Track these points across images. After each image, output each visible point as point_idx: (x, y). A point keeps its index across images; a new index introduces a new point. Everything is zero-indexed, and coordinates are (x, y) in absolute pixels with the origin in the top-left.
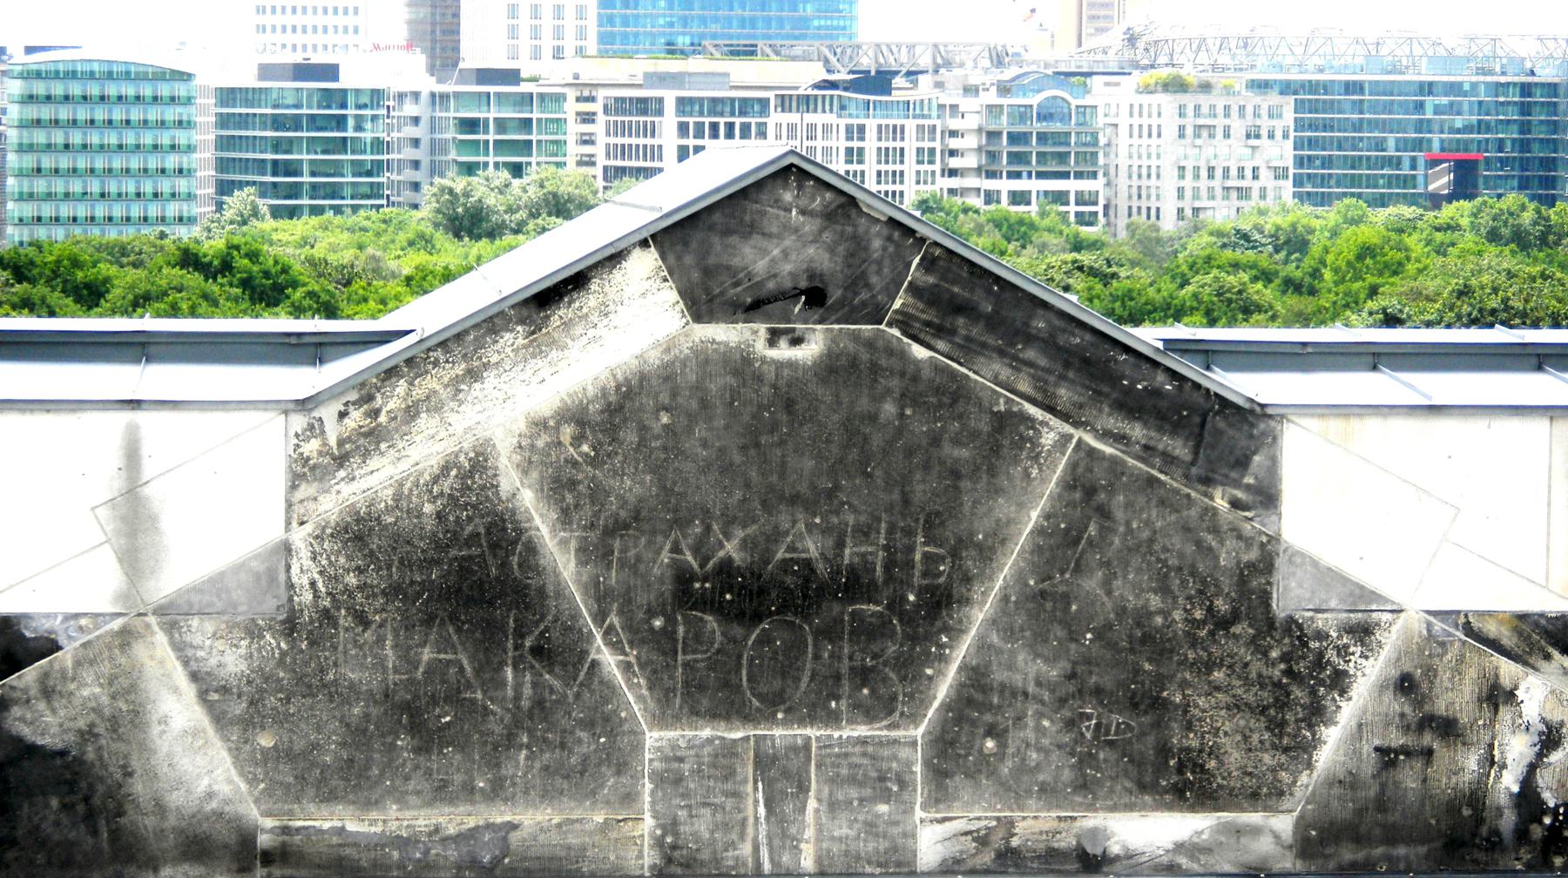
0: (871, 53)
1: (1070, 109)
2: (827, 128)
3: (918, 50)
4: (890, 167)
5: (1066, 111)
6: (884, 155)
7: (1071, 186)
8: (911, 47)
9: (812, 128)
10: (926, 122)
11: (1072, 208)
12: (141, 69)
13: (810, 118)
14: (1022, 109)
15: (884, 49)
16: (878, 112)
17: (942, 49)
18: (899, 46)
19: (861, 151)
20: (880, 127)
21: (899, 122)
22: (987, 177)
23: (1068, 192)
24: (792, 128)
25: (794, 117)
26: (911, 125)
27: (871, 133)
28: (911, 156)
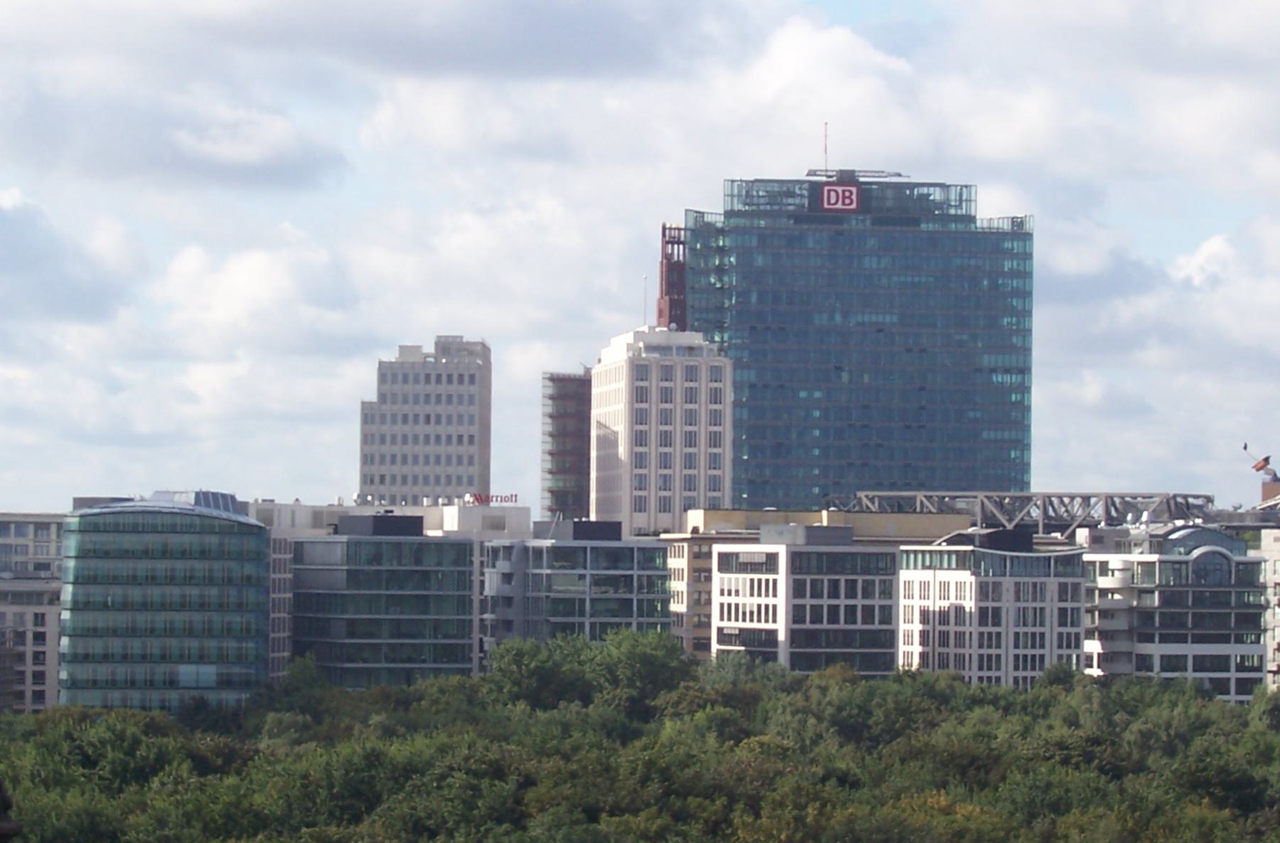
1: (1230, 566)
2: (960, 586)
5: (1225, 567)
6: (1022, 617)
8: (1086, 499)
11: (1233, 675)
12: (207, 522)
13: (943, 575)
14: (1177, 566)
15: (1055, 501)
16: (1015, 568)
17: (1117, 500)
18: (1072, 498)
19: (996, 612)
20: (1017, 584)
21: (1039, 580)
22: (1140, 641)
23: (1186, 656)
24: (924, 586)
25: (927, 575)
26: (1052, 583)
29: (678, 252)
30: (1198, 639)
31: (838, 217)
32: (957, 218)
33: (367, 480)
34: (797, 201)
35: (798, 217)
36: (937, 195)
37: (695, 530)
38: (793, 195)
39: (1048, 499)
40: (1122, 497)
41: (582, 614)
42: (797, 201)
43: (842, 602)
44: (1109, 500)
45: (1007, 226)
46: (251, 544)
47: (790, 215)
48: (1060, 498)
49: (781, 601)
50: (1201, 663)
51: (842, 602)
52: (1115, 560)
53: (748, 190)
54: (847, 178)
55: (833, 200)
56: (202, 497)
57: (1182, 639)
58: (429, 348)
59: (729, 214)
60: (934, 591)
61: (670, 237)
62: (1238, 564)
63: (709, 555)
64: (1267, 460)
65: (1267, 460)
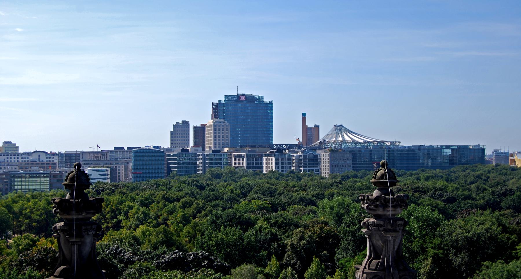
0: (276, 146)
2: (272, 159)
3: (284, 146)
4: (283, 166)
7: (314, 168)
8: (283, 145)
9: (269, 159)
10: (289, 158)
13: (269, 157)
18: (281, 145)
20: (281, 159)
25: (266, 157)
27: (280, 160)
28: (286, 164)
29: (215, 107)
30: (309, 167)
31: (242, 101)
32: (261, 101)
33: (171, 143)
34: (236, 98)
35: (236, 101)
36: (257, 97)
37: (228, 151)
38: (235, 98)
39: (277, 145)
40: (289, 145)
41: (214, 164)
42: (236, 98)
43: (254, 162)
44: (287, 145)
45: (269, 102)
46: (162, 154)
47: (235, 101)
48: (279, 145)
49: (245, 163)
50: (309, 170)
51: (254, 162)
52: (295, 154)
53: (226, 97)
54: (243, 95)
55: (241, 98)
56: (154, 147)
57: (306, 167)
58: (181, 122)
59: (225, 101)
60: (268, 160)
61: (213, 104)
62: (315, 155)
63: (231, 155)
64: (298, 139)
65: (298, 139)
